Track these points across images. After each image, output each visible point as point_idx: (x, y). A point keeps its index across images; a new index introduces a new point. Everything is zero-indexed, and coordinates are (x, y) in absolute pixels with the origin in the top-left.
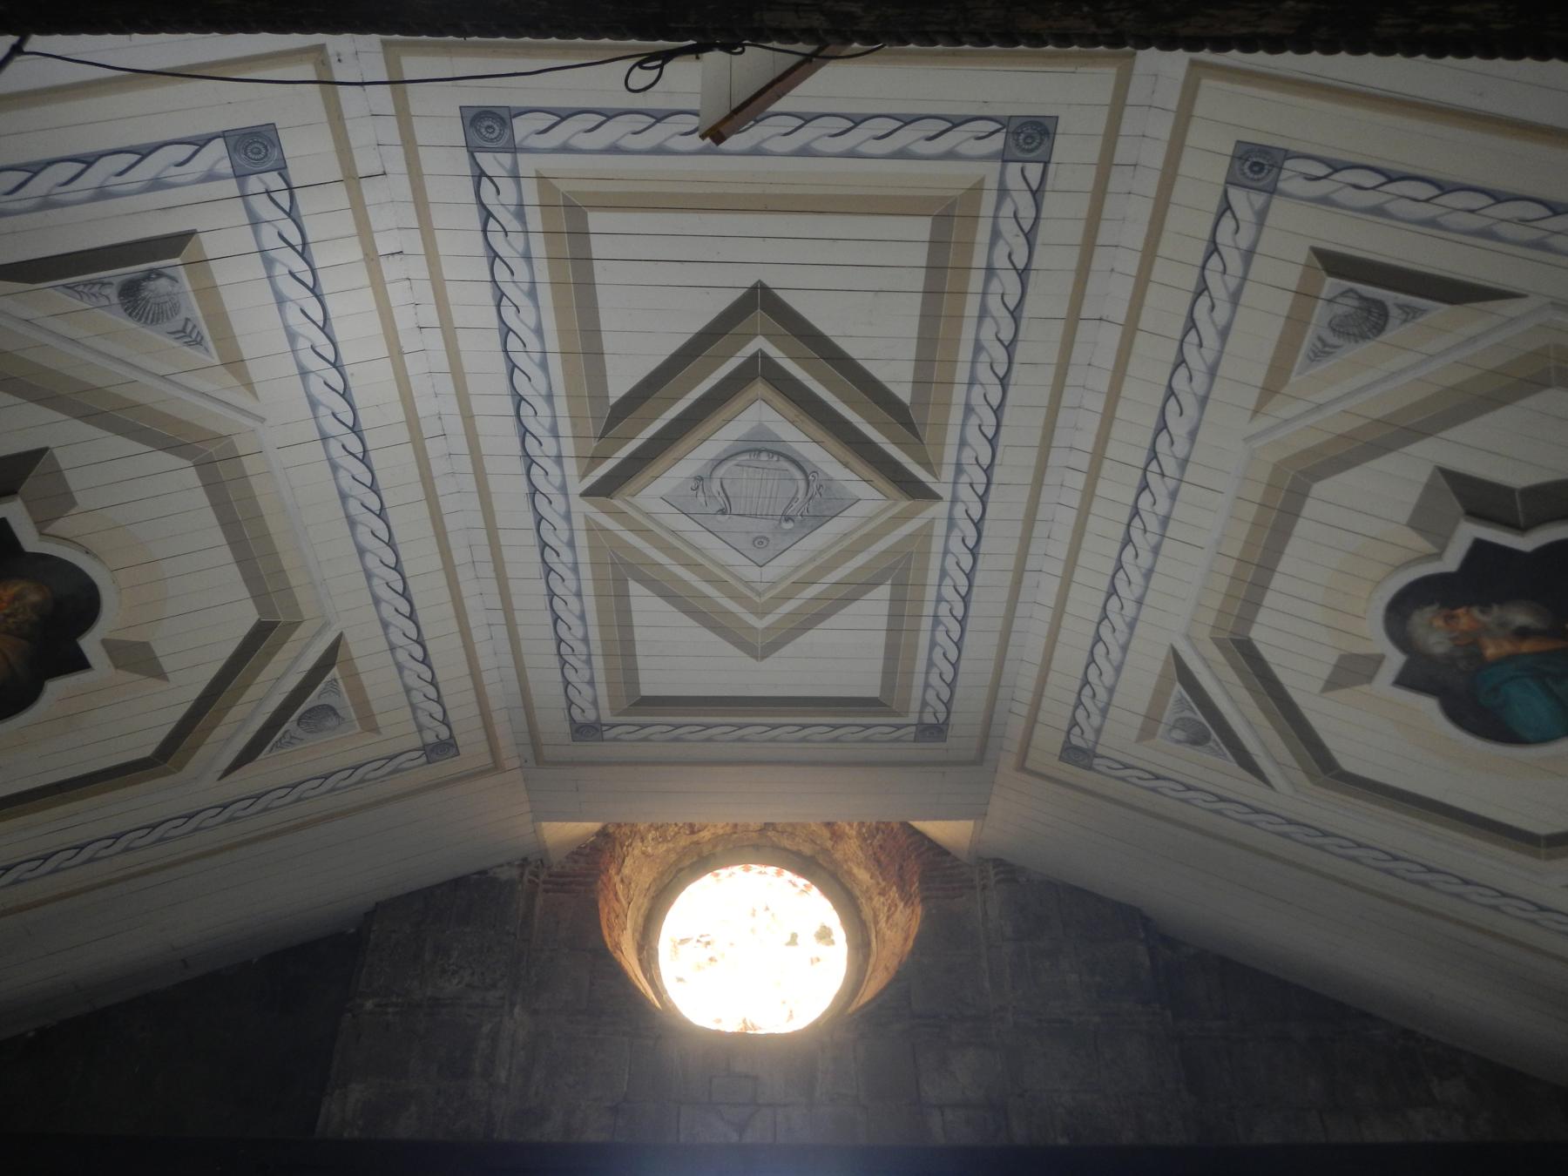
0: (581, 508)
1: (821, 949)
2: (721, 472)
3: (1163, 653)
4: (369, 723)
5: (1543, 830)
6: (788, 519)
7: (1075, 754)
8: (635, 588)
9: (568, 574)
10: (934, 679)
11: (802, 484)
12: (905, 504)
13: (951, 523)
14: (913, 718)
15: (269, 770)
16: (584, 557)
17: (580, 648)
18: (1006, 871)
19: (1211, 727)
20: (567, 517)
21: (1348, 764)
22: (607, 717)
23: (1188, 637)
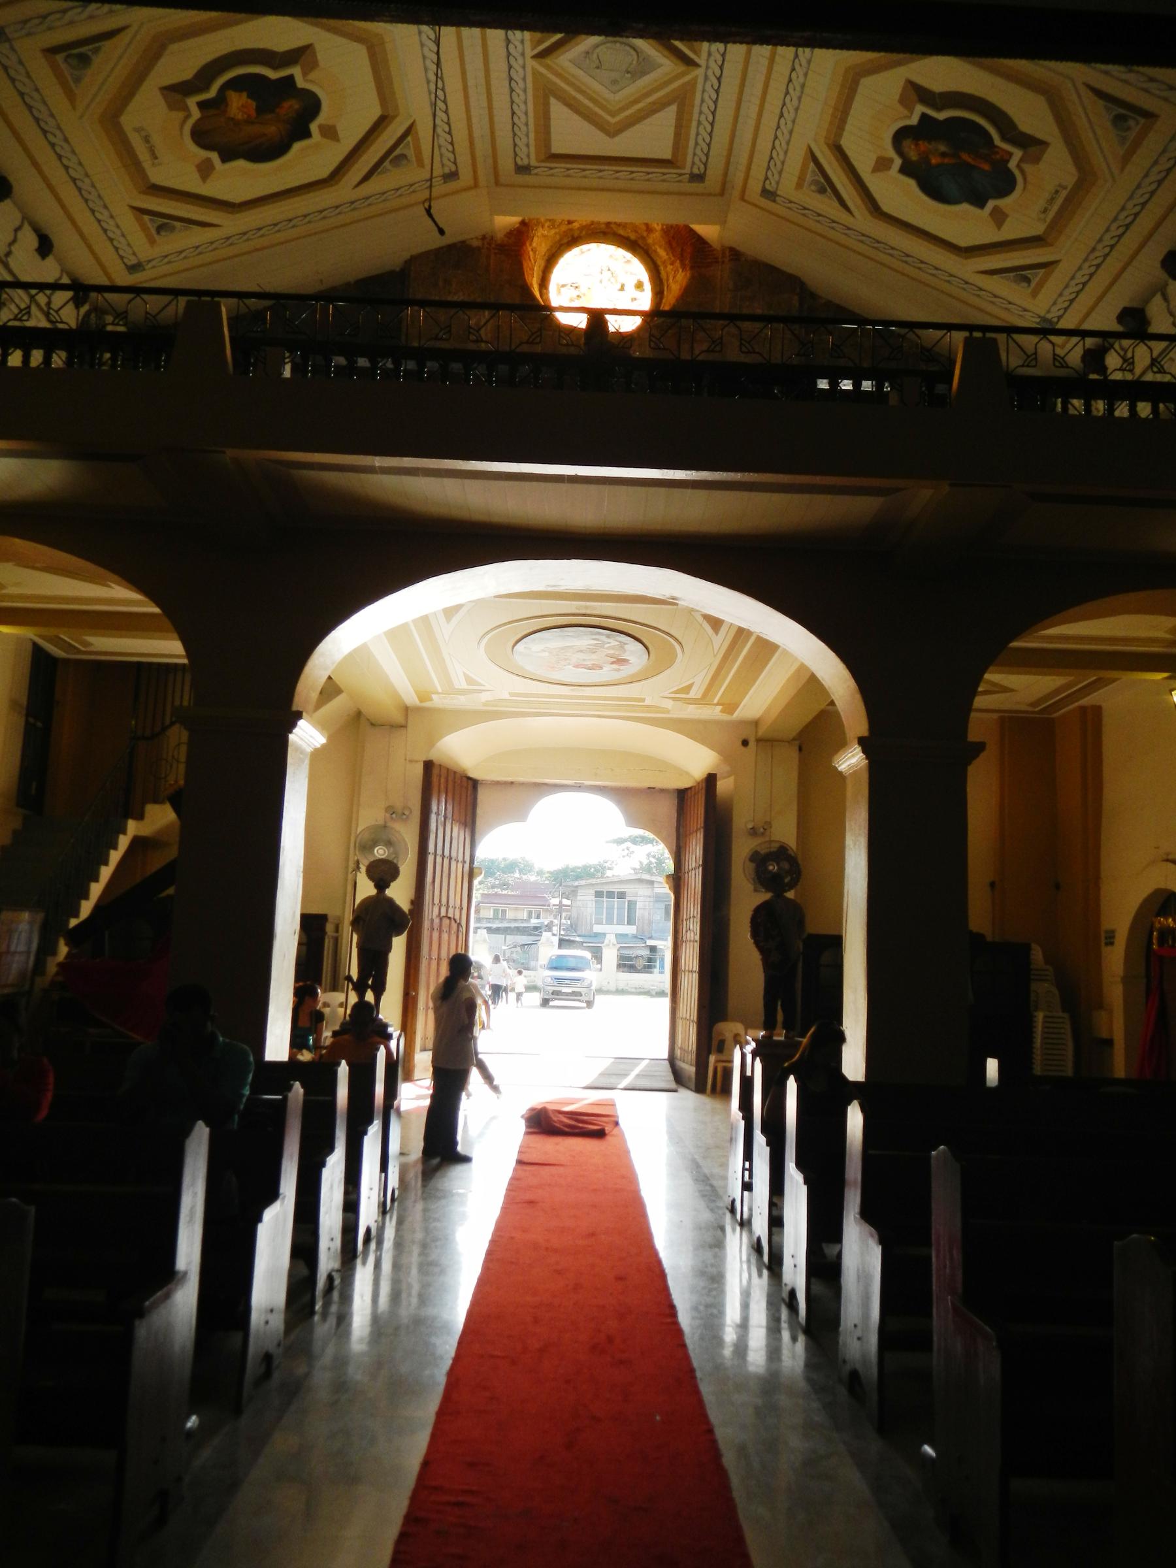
0: (531, 64)
1: (637, 294)
2: (598, 50)
3: (805, 148)
4: (420, 163)
5: (963, 243)
6: (628, 72)
7: (765, 193)
8: (553, 100)
9: (521, 93)
10: (698, 152)
11: (635, 57)
12: (682, 68)
13: (706, 78)
14: (687, 170)
15: (375, 185)
16: (530, 85)
17: (524, 128)
18: (735, 254)
19: (826, 186)
20: (524, 67)
21: (885, 209)
22: (533, 163)
23: (815, 140)
